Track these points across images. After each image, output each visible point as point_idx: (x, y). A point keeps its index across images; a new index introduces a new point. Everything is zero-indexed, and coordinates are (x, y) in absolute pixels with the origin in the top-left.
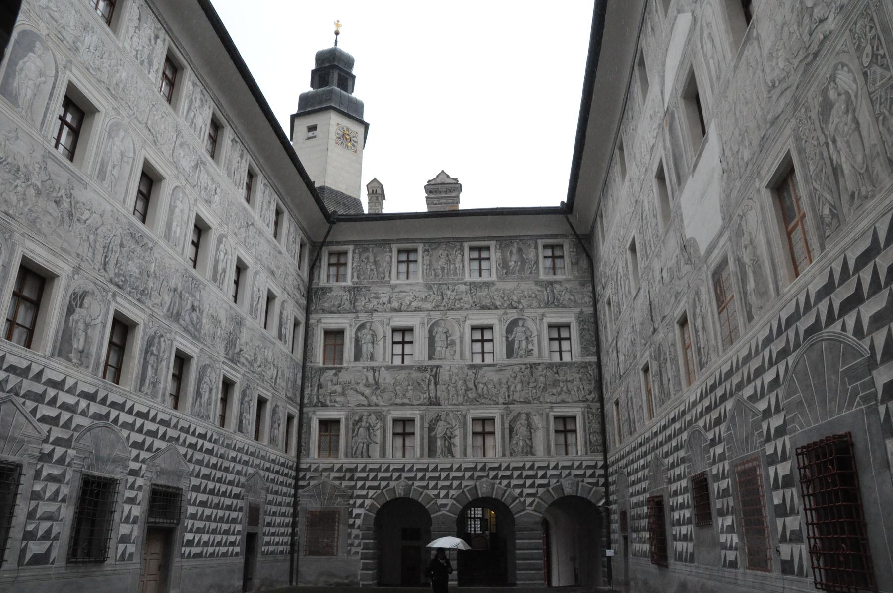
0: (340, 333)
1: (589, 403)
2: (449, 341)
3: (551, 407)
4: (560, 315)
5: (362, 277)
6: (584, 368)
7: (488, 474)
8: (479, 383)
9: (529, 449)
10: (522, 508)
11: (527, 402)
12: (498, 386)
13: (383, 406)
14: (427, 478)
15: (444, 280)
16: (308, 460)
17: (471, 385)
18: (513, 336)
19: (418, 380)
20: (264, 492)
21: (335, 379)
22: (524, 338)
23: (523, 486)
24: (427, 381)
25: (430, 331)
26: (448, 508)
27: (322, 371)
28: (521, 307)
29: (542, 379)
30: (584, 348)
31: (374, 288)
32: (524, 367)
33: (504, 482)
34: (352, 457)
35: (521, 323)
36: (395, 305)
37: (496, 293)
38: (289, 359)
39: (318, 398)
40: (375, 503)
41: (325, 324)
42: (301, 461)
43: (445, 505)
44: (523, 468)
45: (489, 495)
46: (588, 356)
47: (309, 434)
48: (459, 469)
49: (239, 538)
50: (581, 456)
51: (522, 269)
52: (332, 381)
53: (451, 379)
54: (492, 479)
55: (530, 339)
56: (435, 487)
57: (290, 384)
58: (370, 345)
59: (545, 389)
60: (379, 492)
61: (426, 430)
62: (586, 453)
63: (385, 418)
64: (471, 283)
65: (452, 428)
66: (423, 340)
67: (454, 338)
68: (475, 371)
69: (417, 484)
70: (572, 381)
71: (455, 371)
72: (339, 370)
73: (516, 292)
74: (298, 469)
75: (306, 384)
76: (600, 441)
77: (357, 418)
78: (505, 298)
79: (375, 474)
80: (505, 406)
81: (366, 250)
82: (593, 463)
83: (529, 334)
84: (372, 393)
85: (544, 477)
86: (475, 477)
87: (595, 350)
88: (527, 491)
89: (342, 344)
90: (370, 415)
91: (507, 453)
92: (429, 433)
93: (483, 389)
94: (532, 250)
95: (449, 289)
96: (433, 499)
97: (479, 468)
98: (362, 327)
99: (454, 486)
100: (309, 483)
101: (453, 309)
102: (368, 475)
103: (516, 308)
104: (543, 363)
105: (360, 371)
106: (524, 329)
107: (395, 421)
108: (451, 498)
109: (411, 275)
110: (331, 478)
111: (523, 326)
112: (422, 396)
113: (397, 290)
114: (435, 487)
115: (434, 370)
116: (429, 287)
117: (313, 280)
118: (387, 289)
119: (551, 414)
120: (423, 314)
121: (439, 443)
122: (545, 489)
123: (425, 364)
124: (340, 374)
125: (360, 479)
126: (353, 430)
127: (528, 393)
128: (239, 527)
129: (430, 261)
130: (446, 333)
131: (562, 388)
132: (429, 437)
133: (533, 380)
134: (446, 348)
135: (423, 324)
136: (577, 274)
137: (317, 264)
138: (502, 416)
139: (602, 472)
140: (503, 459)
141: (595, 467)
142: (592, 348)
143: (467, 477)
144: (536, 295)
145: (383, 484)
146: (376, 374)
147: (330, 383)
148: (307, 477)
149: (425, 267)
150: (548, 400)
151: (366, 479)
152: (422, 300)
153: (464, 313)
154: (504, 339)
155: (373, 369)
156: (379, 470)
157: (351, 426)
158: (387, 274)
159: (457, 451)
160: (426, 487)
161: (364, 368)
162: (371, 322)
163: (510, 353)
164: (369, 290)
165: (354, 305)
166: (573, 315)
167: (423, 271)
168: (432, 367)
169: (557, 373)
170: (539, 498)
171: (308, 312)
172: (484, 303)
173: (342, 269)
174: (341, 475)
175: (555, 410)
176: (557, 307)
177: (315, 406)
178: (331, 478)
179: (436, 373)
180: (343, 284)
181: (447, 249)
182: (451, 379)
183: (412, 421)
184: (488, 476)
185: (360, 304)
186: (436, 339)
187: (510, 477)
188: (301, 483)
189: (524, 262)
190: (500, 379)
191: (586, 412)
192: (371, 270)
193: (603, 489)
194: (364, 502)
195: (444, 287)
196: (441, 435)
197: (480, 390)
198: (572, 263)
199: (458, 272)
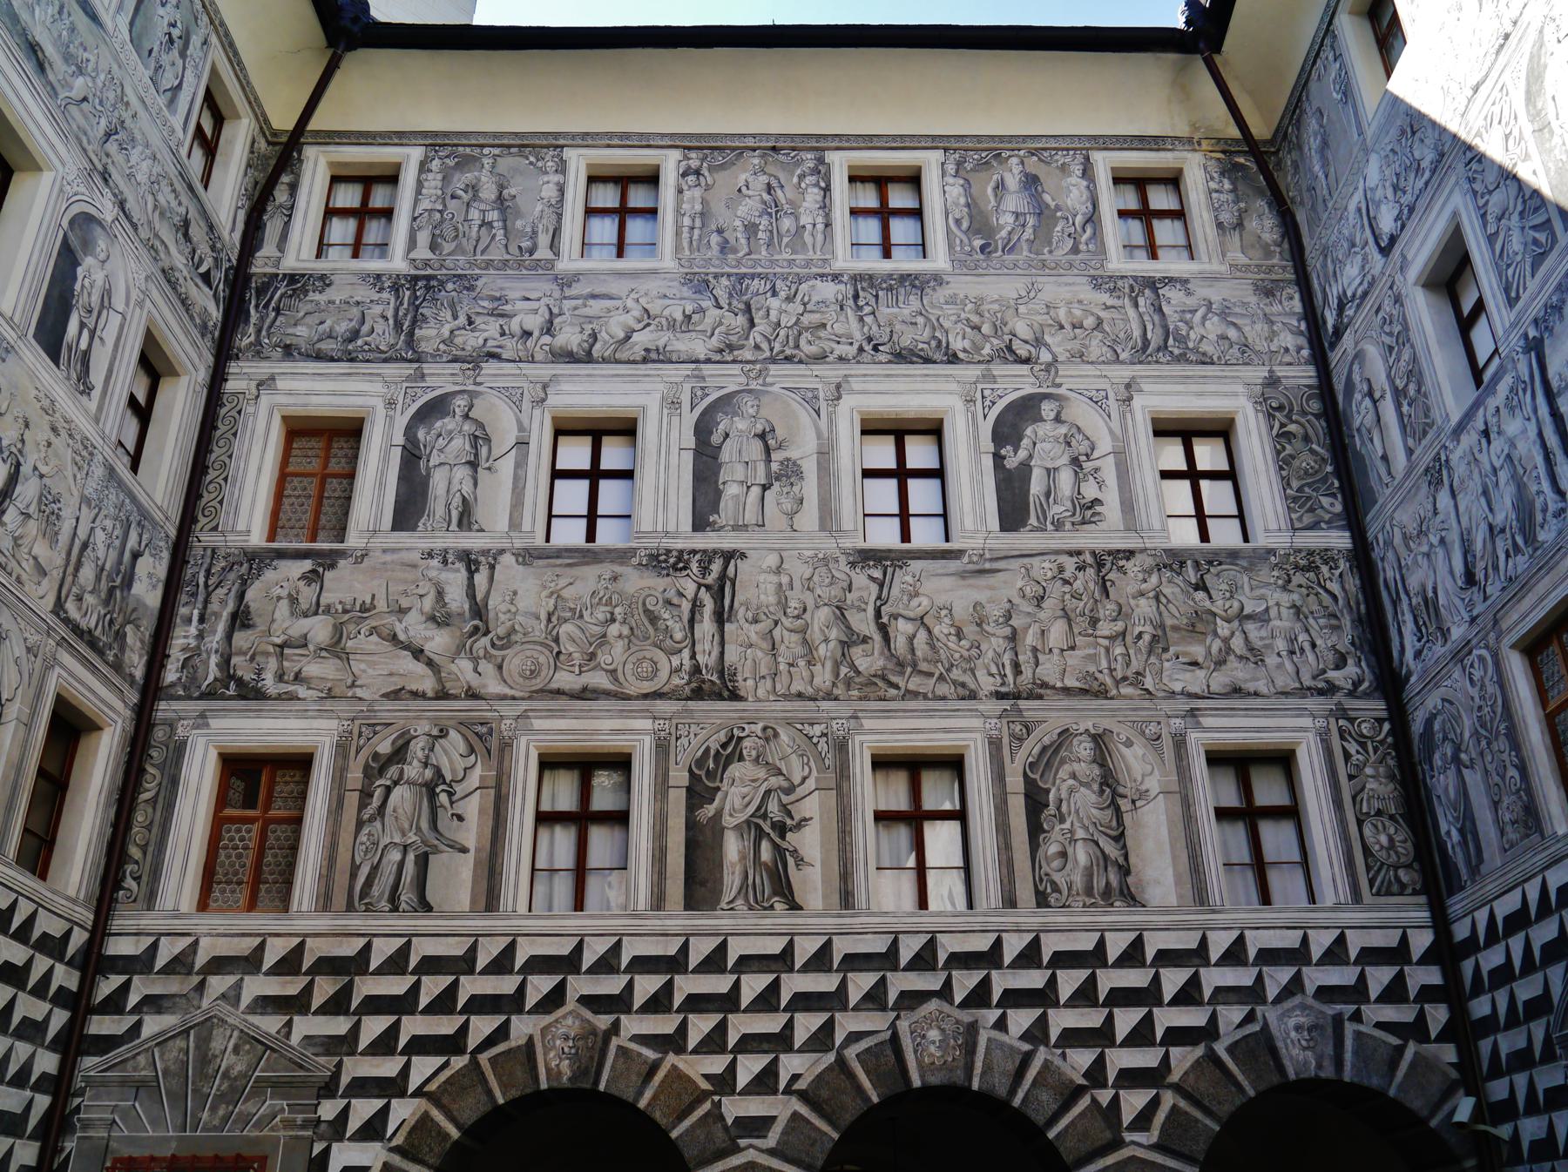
0: (349, 431)
1: (1339, 697)
2: (775, 467)
4: (1194, 388)
5: (448, 247)
6: (1297, 567)
7: (948, 984)
8: (895, 617)
9: (1114, 878)
10: (1108, 1135)
11: (1092, 691)
12: (970, 630)
13: (504, 698)
14: (678, 1000)
16: (149, 921)
17: (863, 623)
18: (1022, 454)
19: (650, 602)
21: (307, 594)
22: (1065, 460)
23: (1102, 1036)
24: (686, 606)
25: (703, 430)
26: (772, 1140)
27: (256, 561)
28: (1045, 357)
29: (1145, 607)
30: (1295, 500)
31: (489, 283)
32: (1070, 563)
33: (1021, 1019)
34: (350, 907)
35: (1048, 409)
36: (570, 337)
37: (951, 310)
38: (99, 472)
39: (225, 662)
40: (436, 1114)
41: (290, 393)
42: (117, 924)
43: (758, 1126)
44: (1097, 957)
45: (958, 1077)
46: (1314, 526)
47: (170, 807)
48: (820, 961)
50: (1337, 907)
51: (1043, 236)
52: (293, 600)
53: (783, 604)
54: (964, 1005)
55: (1088, 466)
56: (714, 1042)
57: (87, 573)
58: (462, 473)
59: (1159, 643)
60: (459, 1062)
61: (677, 799)
62: (1357, 896)
63: (506, 746)
64: (856, 278)
67: (793, 454)
69: (633, 1025)
70: (1262, 618)
71: (799, 570)
72: (329, 560)
73: (1022, 309)
74: (93, 962)
75: (183, 611)
76: (1405, 849)
77: (385, 748)
78: (986, 329)
79: (445, 981)
80: (1006, 704)
81: (465, 163)
82: (1390, 939)
84: (460, 648)
85: (1188, 995)
86: (892, 996)
87: (1338, 508)
88: (1121, 1059)
89: (351, 476)
90: (443, 733)
91: (1025, 892)
93: (911, 639)
94: (1075, 179)
95: (775, 294)
96: (703, 1096)
97: (905, 956)
98: (435, 408)
99: (800, 1037)
100: (136, 1028)
101: (788, 359)
102: (415, 989)
103: (1027, 361)
105: (415, 566)
106: (1063, 430)
108: (788, 1091)
110: (246, 999)
111: (1058, 419)
113: (576, 290)
114: (714, 1042)
115: (716, 567)
116: (701, 284)
117: (259, 247)
118: (541, 287)
119: (1197, 743)
121: (733, 848)
122: (1199, 1051)
124: (329, 575)
125: (375, 1005)
126: (366, 795)
127: (1092, 658)
129: (704, 202)
130: (762, 436)
132: (691, 825)
133: (1109, 608)
134: (765, 488)
135: (675, 404)
136: (1242, 259)
137: (281, 195)
138: (995, 745)
139: (1432, 976)
140: (1009, 919)
141: (1398, 954)
142: (1325, 501)
143: (854, 997)
144: (1100, 322)
145: (483, 1026)
146: (481, 579)
147: (283, 608)
148: (133, 999)
149: (687, 221)
150: (1178, 687)
151: (403, 1005)
152: (672, 325)
153: (832, 372)
154: (988, 462)
155: (470, 561)
156: (465, 965)
157: (355, 776)
158: (544, 240)
159: (812, 883)
160: (675, 1042)
161: (430, 555)
162: (473, 395)
163: (1013, 512)
164: (471, 288)
165: (411, 334)
166: (1240, 388)
167: (678, 234)
168: (707, 557)
170: (1177, 1088)
171: (224, 353)
172: (906, 342)
174: (291, 986)
175: (1207, 721)
176: (1181, 359)
177: (209, 695)
178: (246, 999)
179: (723, 576)
181: (770, 169)
182: (783, 604)
183: (621, 763)
184: (946, 992)
185: (429, 337)
186: (725, 455)
187: (1044, 997)
188: (100, 1025)
189: (1044, 214)
192: (486, 224)
193: (1449, 1053)
194: (385, 1111)
196: (742, 817)
197: (900, 644)
198: (1220, 225)
199: (807, 237)
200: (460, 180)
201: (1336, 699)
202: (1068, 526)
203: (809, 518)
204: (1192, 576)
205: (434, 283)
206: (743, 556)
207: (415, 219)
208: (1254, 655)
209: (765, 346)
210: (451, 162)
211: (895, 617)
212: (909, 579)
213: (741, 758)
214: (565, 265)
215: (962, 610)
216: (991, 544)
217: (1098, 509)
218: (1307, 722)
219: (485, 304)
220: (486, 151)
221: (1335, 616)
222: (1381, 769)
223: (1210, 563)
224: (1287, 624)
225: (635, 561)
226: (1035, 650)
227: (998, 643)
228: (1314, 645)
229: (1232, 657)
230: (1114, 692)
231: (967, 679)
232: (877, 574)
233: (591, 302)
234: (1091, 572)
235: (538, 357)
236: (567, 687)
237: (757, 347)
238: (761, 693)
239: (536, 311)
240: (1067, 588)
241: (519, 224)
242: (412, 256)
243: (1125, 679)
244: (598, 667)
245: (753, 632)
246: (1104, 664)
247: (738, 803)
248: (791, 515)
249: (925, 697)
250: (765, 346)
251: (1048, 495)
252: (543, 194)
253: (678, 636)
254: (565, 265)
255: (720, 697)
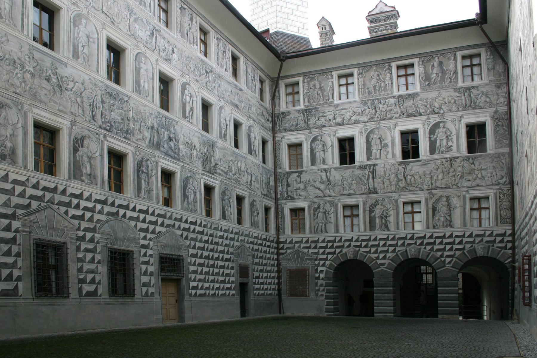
1: (500, 185)
2: (383, 145)
3: (468, 191)
5: (312, 101)
8: (407, 175)
12: (423, 177)
15: (376, 96)
17: (401, 177)
18: (435, 136)
19: (360, 176)
20: (250, 258)
22: (445, 137)
24: (367, 176)
25: (367, 138)
29: (460, 169)
31: (321, 108)
32: (444, 161)
36: (339, 120)
49: (233, 285)
53: (385, 174)
55: (450, 138)
59: (462, 177)
61: (367, 212)
65: (388, 210)
66: (362, 146)
67: (386, 142)
68: (404, 166)
70: (485, 170)
71: (388, 167)
80: (429, 191)
81: (312, 79)
83: (449, 134)
92: (370, 214)
95: (381, 103)
101: (384, 119)
104: (460, 157)
107: (344, 207)
109: (350, 96)
112: (363, 188)
115: (372, 168)
116: (364, 103)
120: (361, 125)
123: (365, 164)
127: (448, 181)
128: (232, 279)
130: (380, 138)
131: (477, 175)
133: (452, 170)
134: (381, 150)
135: (361, 133)
137: (277, 94)
150: (465, 185)
152: (359, 114)
153: (394, 121)
154: (428, 139)
158: (331, 97)
162: (321, 135)
163: (433, 150)
164: (317, 111)
165: (308, 123)
167: (359, 91)
168: (370, 166)
169: (473, 163)
173: (296, 96)
179: (373, 169)
180: (298, 108)
182: (385, 174)
183: (357, 206)
186: (372, 144)
190: (424, 171)
191: (498, 193)
192: (318, 94)
195: (377, 101)
196: (379, 215)
197: (408, 180)
200: (312, 83)
201: (499, 186)
202: (444, 152)
203: (390, 156)
204: (471, 161)
205: (310, 110)
206: (377, 165)
207: (304, 95)
208: (483, 178)
209: (379, 117)
210: (309, 80)
211: (407, 175)
212: (410, 167)
213: (378, 205)
214: (337, 101)
215: (421, 172)
216: (428, 158)
217: (451, 148)
218: (492, 191)
219: (321, 114)
220: (316, 75)
221: (502, 168)
222: (507, 200)
223: (475, 158)
224: (491, 170)
225: (356, 168)
226: (436, 180)
227: (428, 179)
228: (496, 175)
229: (478, 179)
230: (452, 187)
231: (422, 187)
232: (404, 166)
233: (342, 111)
234: (449, 162)
235: (333, 125)
236: (346, 193)
237: (378, 117)
238: (382, 192)
239: (331, 114)
240: (443, 166)
241: (325, 93)
242: (305, 104)
243: (454, 184)
244: (351, 190)
245: (380, 180)
246: (450, 182)
247: (378, 213)
248: (386, 155)
249: (413, 191)
250: (379, 117)
251: (440, 145)
252: (329, 85)
253: (366, 182)
254: (337, 101)
255: (374, 194)
